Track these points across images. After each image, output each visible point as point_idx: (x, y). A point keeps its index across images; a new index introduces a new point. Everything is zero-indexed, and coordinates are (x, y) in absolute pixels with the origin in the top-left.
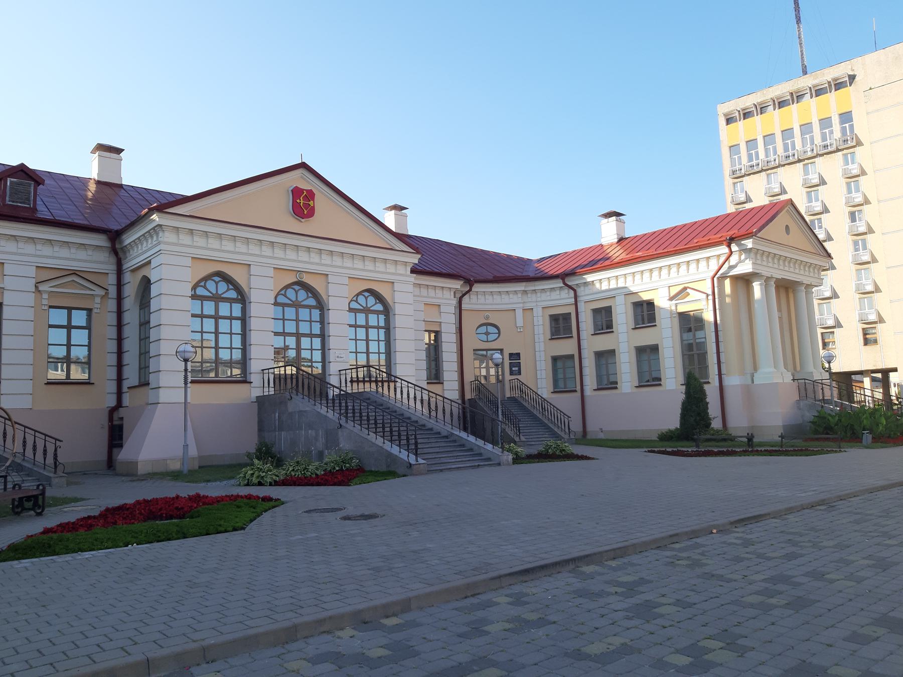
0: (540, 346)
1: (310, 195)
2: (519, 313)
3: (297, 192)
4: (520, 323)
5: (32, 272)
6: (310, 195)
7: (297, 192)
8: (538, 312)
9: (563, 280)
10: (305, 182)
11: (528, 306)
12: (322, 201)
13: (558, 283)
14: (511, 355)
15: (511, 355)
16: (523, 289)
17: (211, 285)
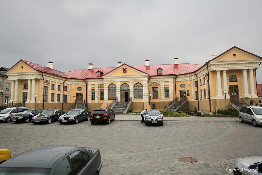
0: (193, 89)
1: (126, 68)
2: (189, 81)
3: (123, 69)
4: (189, 84)
5: (98, 85)
6: (126, 68)
7: (123, 69)
8: (192, 80)
9: (194, 73)
10: (125, 67)
11: (190, 79)
12: (129, 70)
13: (193, 74)
14: (187, 91)
15: (187, 91)
16: (189, 75)
17: (111, 85)
